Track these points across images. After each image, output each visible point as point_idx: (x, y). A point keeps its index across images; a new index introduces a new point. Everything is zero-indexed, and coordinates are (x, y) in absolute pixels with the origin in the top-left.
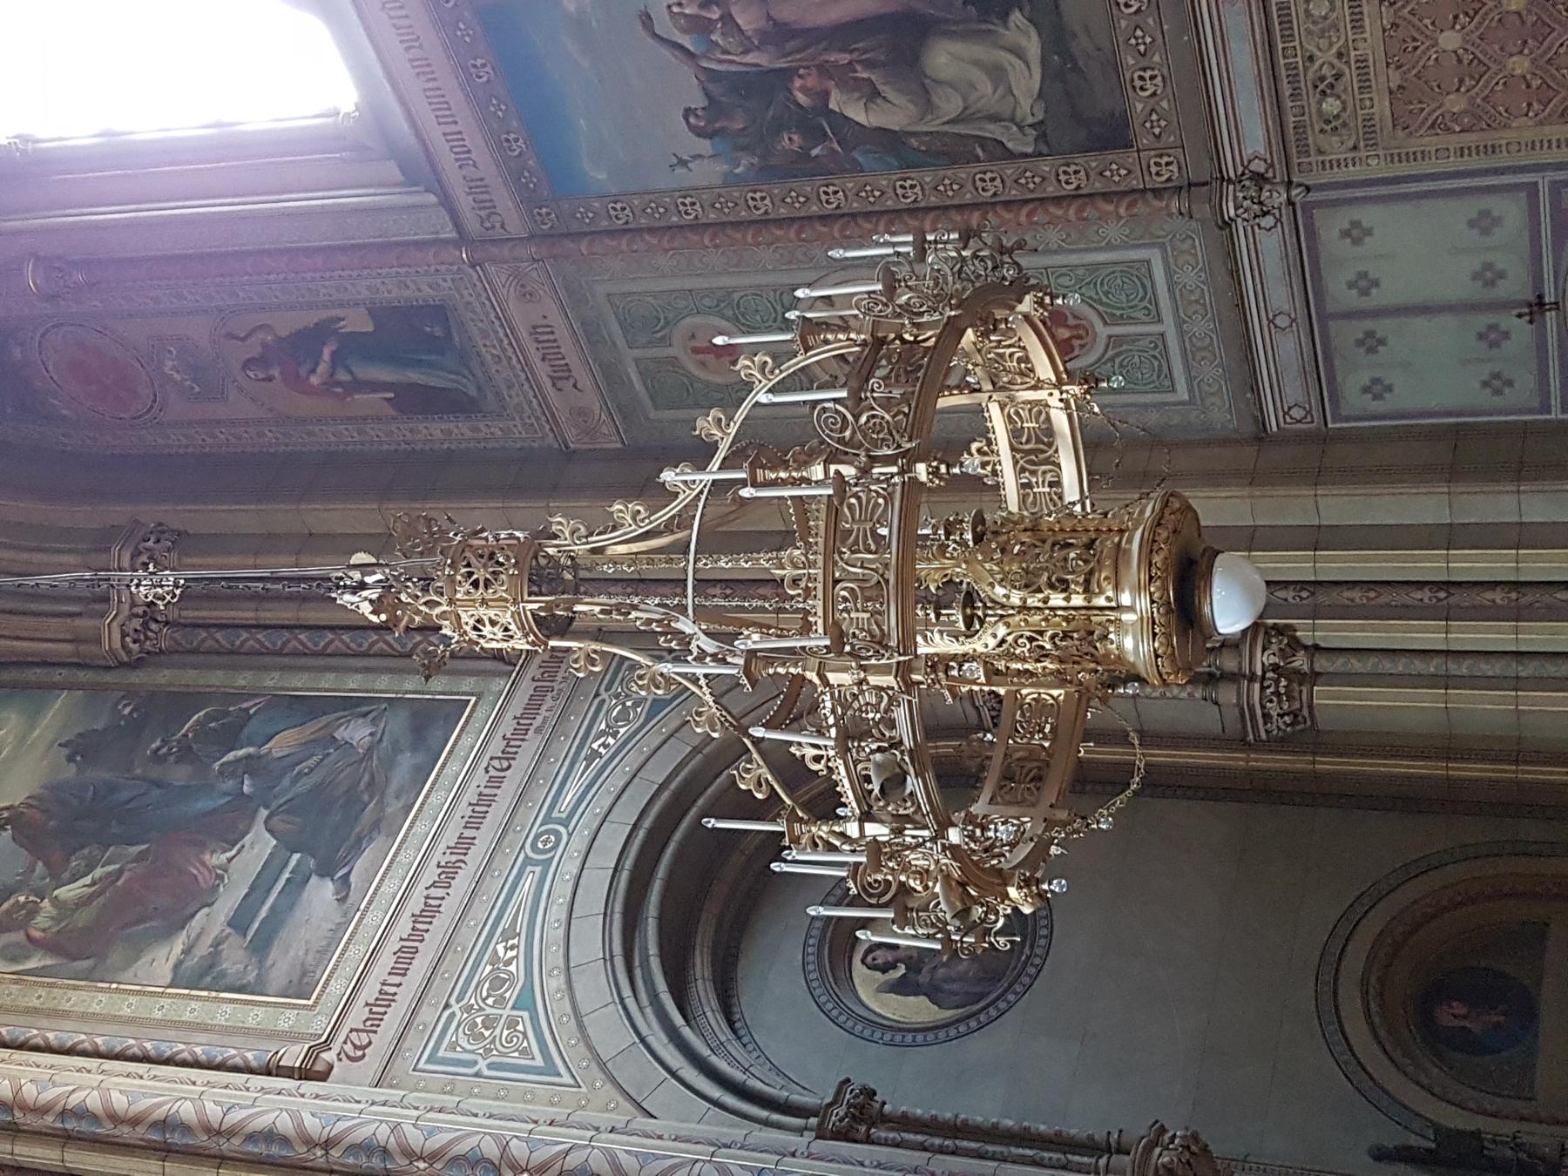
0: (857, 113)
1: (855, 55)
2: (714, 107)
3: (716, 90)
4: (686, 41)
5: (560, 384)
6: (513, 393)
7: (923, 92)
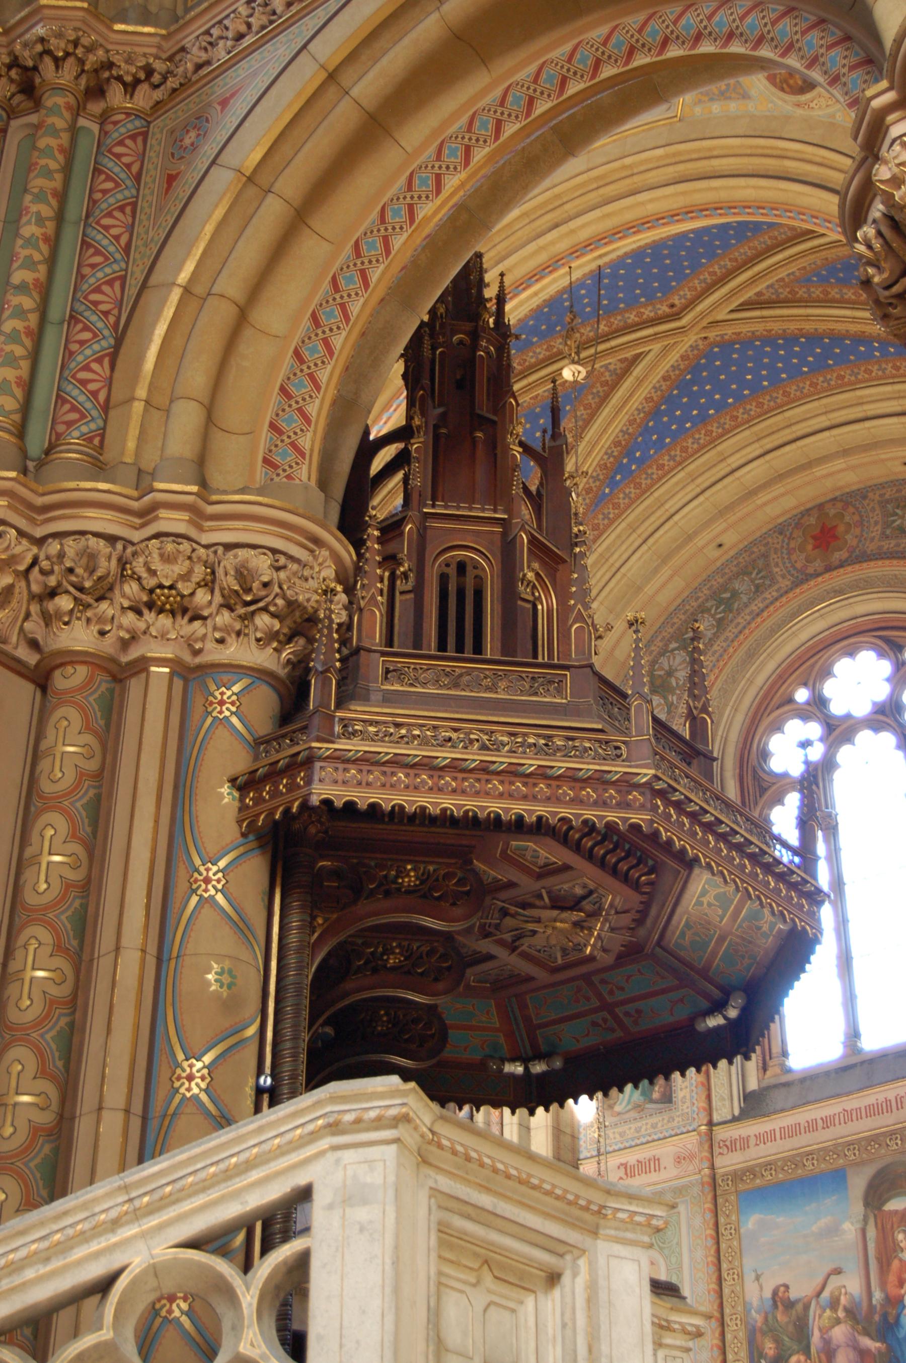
2: (789, 1305)
3: (799, 1307)
4: (826, 1294)
5: (622, 1169)
6: (617, 1136)
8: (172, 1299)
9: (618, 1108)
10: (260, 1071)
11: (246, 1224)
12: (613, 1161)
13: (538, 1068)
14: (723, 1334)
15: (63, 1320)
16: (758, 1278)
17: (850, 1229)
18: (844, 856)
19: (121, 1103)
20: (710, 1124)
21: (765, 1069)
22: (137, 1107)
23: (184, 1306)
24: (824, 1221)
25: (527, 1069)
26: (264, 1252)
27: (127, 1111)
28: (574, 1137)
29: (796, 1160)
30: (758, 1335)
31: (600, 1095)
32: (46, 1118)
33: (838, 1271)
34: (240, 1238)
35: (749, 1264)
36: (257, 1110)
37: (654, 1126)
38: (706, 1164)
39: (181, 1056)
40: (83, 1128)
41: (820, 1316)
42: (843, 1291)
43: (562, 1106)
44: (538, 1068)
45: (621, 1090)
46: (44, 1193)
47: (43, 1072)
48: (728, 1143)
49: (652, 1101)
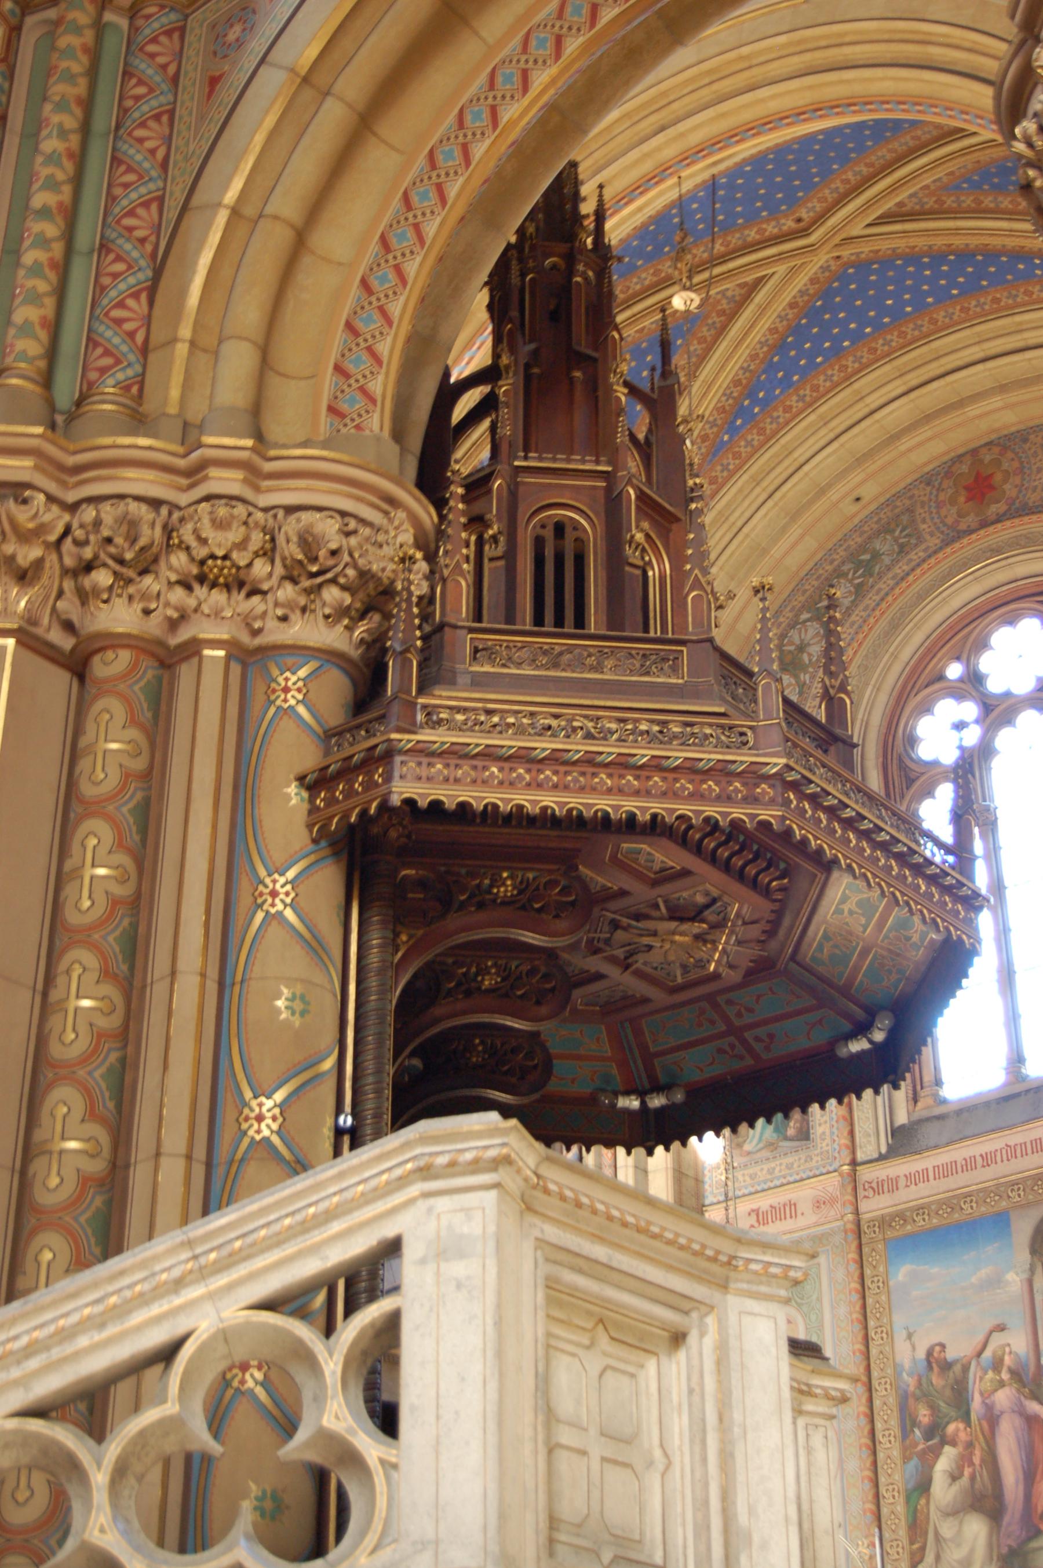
0: (943, 1464)
1: (978, 1468)
2: (946, 1366)
3: (957, 1368)
4: (988, 1354)
5: (754, 1216)
6: (747, 1178)
7: (954, 1512)
8: (244, 1367)
9: (747, 1147)
10: (339, 1110)
11: (327, 1282)
12: (743, 1207)
13: (657, 1102)
14: (870, 1400)
15: (122, 1392)
16: (910, 1336)
17: (1015, 1280)
18: (1004, 855)
19: (182, 1149)
20: (854, 1163)
21: (915, 1100)
22: (200, 1152)
23: (259, 1375)
24: (984, 1272)
25: (643, 1103)
26: (348, 1313)
27: (189, 1157)
28: (699, 1181)
29: (952, 1203)
30: (911, 1401)
31: (727, 1131)
32: (97, 1167)
33: (1001, 1328)
34: (321, 1298)
35: (899, 1321)
36: (337, 1153)
37: (789, 1167)
38: (850, 1209)
39: (248, 1094)
40: (139, 1178)
41: (981, 1379)
42: (1007, 1349)
43: (684, 1144)
44: (657, 1102)
45: (752, 1126)
46: (97, 1251)
47: (92, 1114)
48: (874, 1185)
49: (786, 1138)
